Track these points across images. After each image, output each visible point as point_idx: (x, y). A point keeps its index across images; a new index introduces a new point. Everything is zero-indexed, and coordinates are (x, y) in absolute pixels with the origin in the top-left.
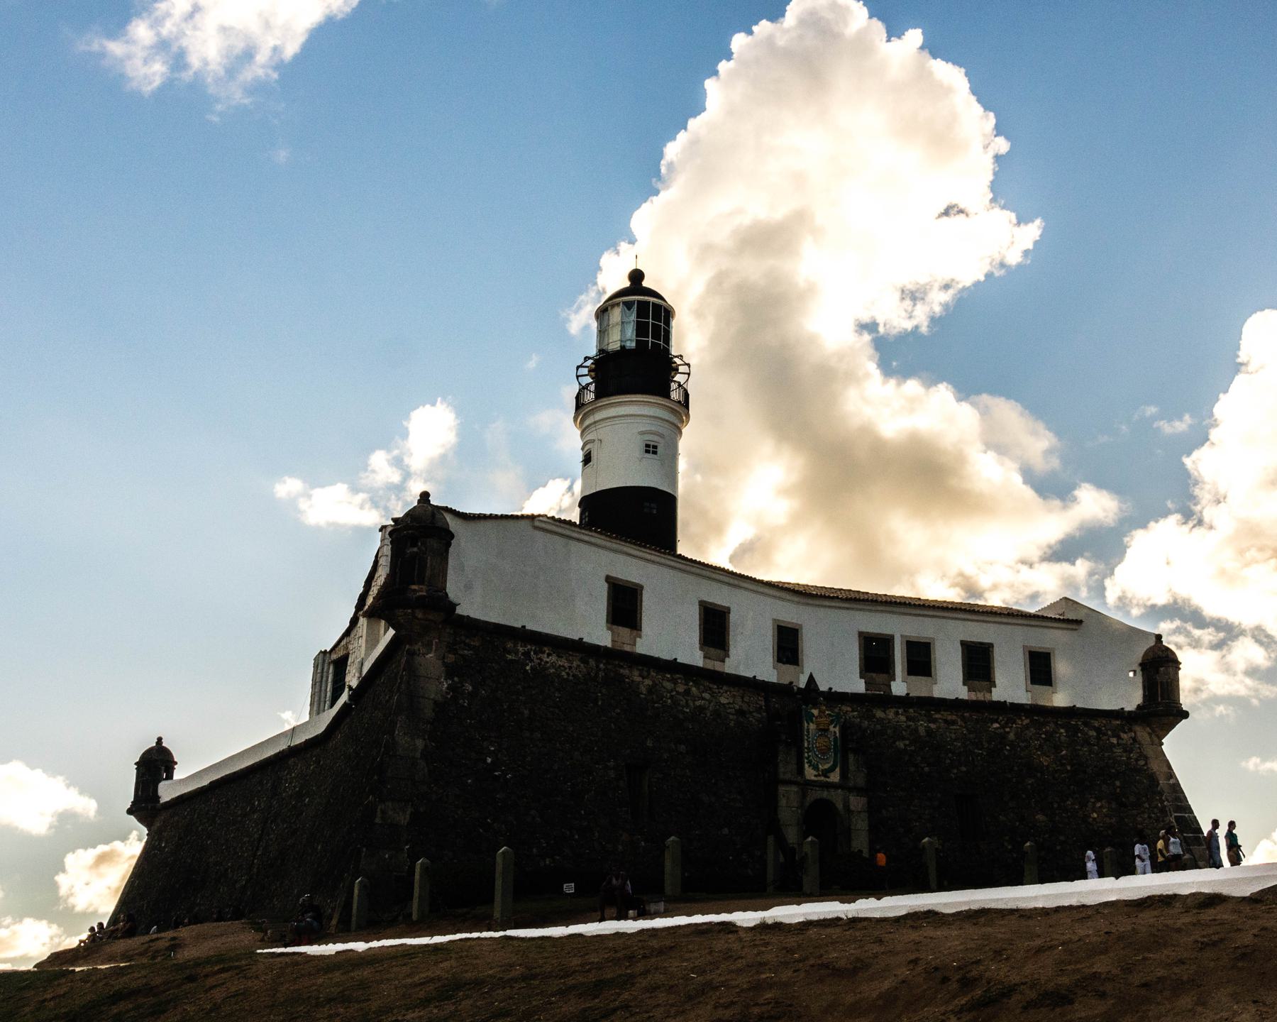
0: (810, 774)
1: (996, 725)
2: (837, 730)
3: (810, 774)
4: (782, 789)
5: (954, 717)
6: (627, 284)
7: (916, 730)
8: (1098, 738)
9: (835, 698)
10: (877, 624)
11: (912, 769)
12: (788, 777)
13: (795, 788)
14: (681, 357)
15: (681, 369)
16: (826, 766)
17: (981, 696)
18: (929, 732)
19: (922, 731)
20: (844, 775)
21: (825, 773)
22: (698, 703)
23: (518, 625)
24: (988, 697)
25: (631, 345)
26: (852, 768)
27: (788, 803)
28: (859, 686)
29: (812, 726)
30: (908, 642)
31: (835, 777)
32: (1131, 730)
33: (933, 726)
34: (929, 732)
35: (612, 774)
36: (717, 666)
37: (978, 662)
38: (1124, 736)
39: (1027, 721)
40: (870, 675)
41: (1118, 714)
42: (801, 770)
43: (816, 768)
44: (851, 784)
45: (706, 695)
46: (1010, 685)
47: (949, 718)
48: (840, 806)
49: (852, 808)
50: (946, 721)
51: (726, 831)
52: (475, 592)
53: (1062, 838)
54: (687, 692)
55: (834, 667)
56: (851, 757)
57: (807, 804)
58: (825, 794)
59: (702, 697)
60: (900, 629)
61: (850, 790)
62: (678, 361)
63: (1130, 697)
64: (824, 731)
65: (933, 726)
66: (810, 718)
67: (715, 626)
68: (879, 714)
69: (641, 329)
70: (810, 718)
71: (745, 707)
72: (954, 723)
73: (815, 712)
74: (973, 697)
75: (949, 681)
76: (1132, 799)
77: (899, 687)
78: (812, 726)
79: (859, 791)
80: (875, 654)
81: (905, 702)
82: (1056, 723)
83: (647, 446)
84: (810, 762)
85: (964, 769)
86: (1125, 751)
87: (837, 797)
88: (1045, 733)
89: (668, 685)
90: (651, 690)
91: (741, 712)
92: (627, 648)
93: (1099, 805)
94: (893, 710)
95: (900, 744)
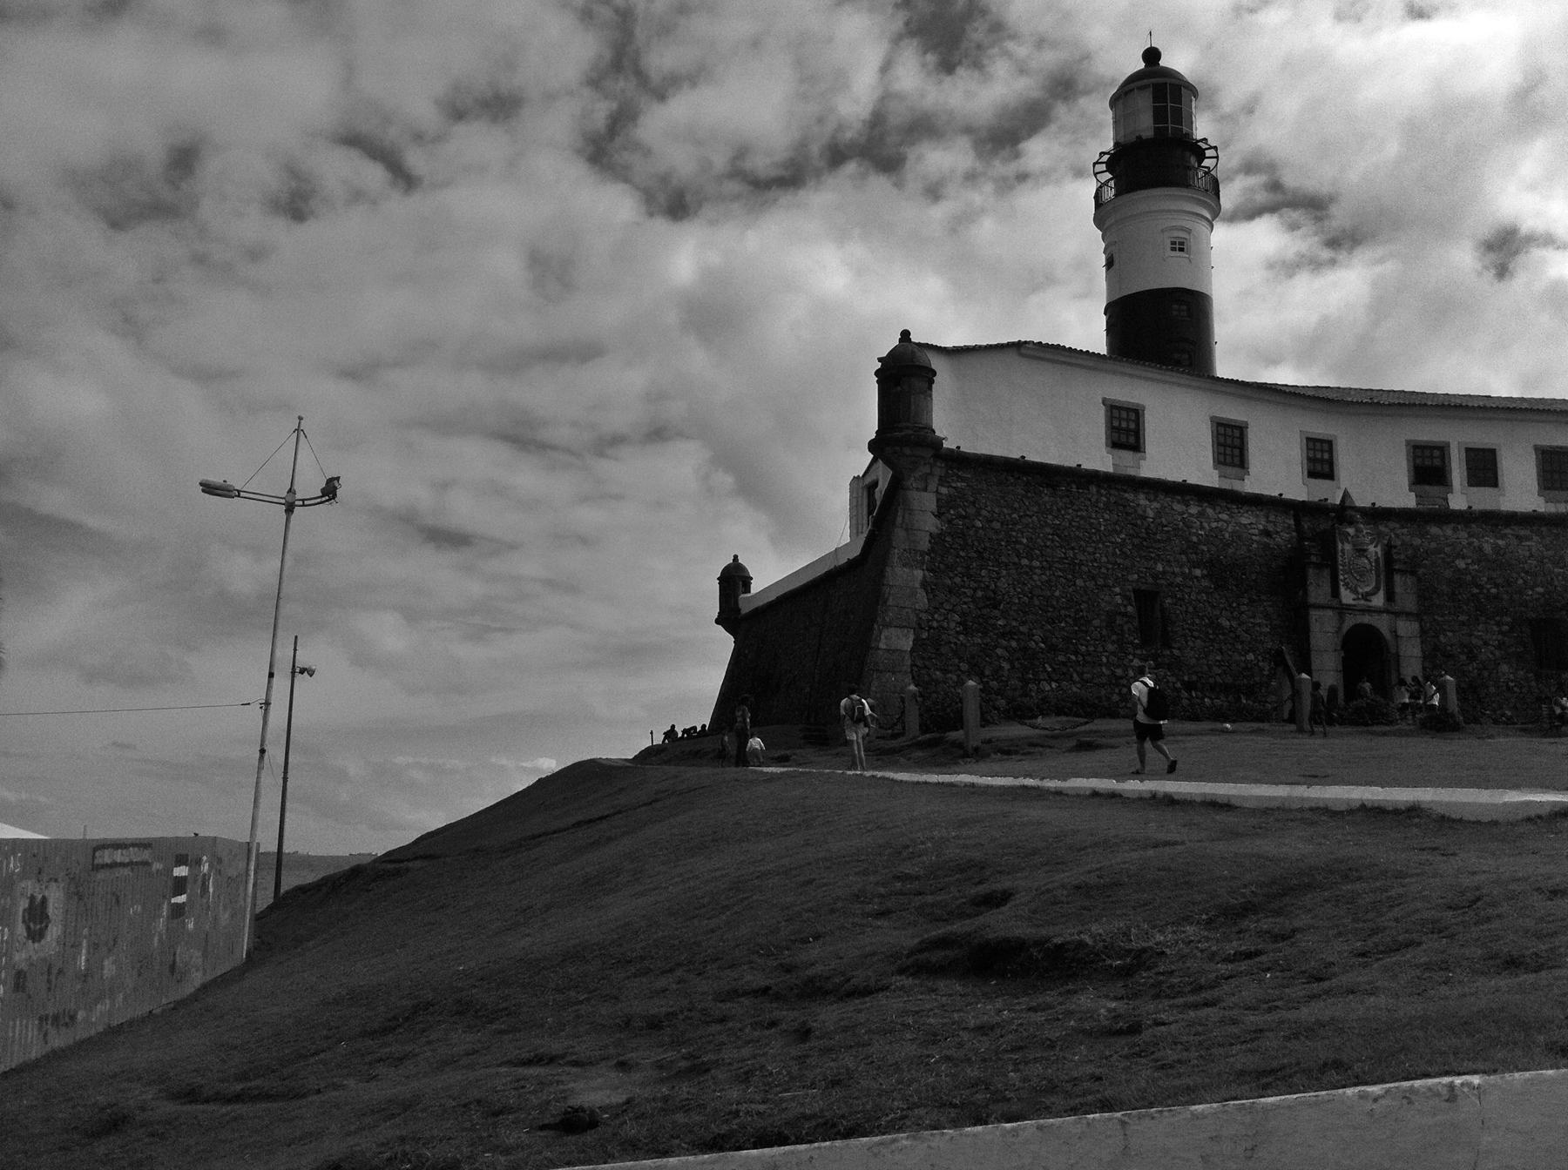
0: (1347, 597)
2: (1379, 549)
3: (1347, 597)
6: (1142, 65)
7: (1481, 549)
9: (1377, 515)
10: (1430, 432)
11: (1476, 591)
12: (1322, 600)
13: (1330, 613)
14: (1205, 140)
15: (1209, 153)
16: (1368, 589)
18: (1497, 549)
19: (1487, 548)
20: (1390, 597)
21: (1366, 596)
22: (1214, 525)
23: (1016, 455)
25: (1148, 133)
26: (1398, 590)
27: (1324, 633)
28: (1408, 500)
29: (1348, 547)
30: (1468, 450)
31: (1378, 600)
33: (1500, 542)
34: (1497, 549)
35: (1118, 599)
36: (1237, 486)
40: (1419, 487)
42: (1335, 593)
43: (1354, 591)
44: (1396, 608)
45: (1224, 516)
47: (1522, 533)
48: (1385, 631)
49: (1400, 633)
51: (1251, 656)
54: (1201, 514)
55: (1375, 476)
56: (1397, 578)
57: (1346, 628)
58: (1366, 619)
59: (1219, 519)
60: (1458, 438)
61: (1397, 614)
62: (1204, 146)
64: (1361, 552)
65: (1500, 542)
67: (1231, 445)
68: (1434, 530)
69: (1159, 115)
71: (1270, 528)
72: (1528, 538)
73: (1351, 531)
74: (1552, 508)
77: (1457, 502)
78: (1348, 547)
79: (1408, 614)
80: (1428, 468)
81: (1467, 518)
84: (1346, 585)
85: (1540, 590)
87: (1382, 623)
89: (1178, 507)
90: (1158, 513)
91: (1266, 533)
92: (1132, 472)
95: (1461, 564)
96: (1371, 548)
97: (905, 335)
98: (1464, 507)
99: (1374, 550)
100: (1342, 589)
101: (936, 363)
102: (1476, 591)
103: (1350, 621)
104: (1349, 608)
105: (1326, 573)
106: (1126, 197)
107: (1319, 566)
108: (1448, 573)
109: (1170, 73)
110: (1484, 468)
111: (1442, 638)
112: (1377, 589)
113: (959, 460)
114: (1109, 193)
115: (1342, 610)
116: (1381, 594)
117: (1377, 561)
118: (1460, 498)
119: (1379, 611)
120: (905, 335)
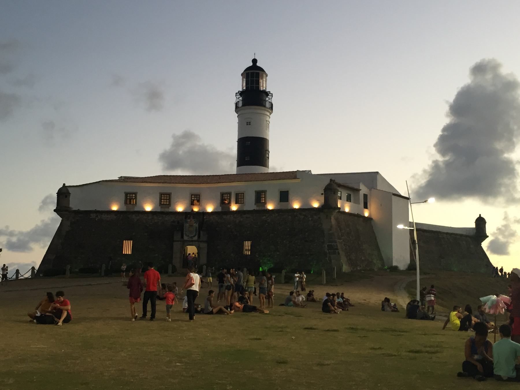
2: (197, 225)
3: (186, 238)
4: (175, 243)
6: (251, 64)
13: (179, 242)
21: (192, 237)
24: (263, 208)
31: (196, 238)
33: (242, 219)
36: (167, 210)
38: (315, 217)
42: (182, 237)
43: (188, 236)
45: (160, 218)
50: (247, 218)
52: (74, 204)
56: (201, 232)
61: (201, 242)
64: (191, 226)
65: (242, 219)
66: (187, 222)
68: (225, 217)
73: (189, 220)
78: (187, 225)
92: (132, 210)
95: (229, 226)
97: (64, 184)
99: (196, 225)
100: (185, 236)
101: (70, 190)
106: (244, 107)
112: (194, 236)
113: (78, 212)
120: (64, 184)
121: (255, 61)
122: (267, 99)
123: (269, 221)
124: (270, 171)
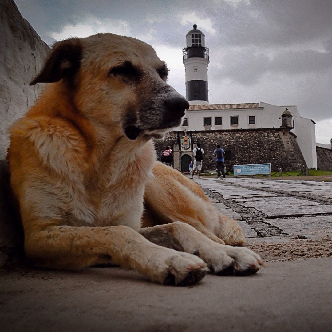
0: (182, 149)
1: (238, 134)
2: (190, 140)
3: (182, 149)
5: (227, 134)
6: (193, 28)
8: (268, 135)
10: (207, 115)
12: (176, 151)
13: (178, 153)
16: (187, 148)
17: (235, 128)
18: (220, 138)
19: (218, 137)
21: (187, 149)
32: (278, 132)
34: (220, 138)
37: (234, 120)
38: (275, 134)
39: (248, 133)
41: (274, 129)
42: (180, 149)
43: (184, 148)
46: (243, 124)
48: (191, 156)
50: (225, 135)
53: (252, 159)
56: (194, 145)
57: (182, 155)
58: (187, 154)
63: (278, 124)
65: (221, 136)
68: (208, 134)
70: (183, 138)
71: (171, 137)
72: (227, 135)
73: (184, 137)
74: (233, 128)
75: (226, 125)
76: (275, 149)
77: (213, 129)
80: (207, 121)
81: (214, 132)
82: (256, 133)
83: (195, 70)
84: (183, 147)
85: (228, 145)
86: (275, 137)
88: (252, 135)
91: (170, 138)
93: (264, 151)
94: (211, 133)
95: (212, 141)
96: (188, 140)
98: (214, 130)
100: (181, 148)
102: (214, 146)
103: (183, 154)
104: (183, 152)
105: (178, 145)
106: (188, 59)
107: (176, 144)
108: (209, 143)
109: (199, 31)
110: (219, 121)
111: (206, 156)
114: (186, 57)
115: (181, 152)
116: (191, 148)
117: (190, 142)
118: (214, 127)
119: (190, 152)
121: (195, 26)
122: (205, 53)
123: (242, 137)
124: (210, 103)
